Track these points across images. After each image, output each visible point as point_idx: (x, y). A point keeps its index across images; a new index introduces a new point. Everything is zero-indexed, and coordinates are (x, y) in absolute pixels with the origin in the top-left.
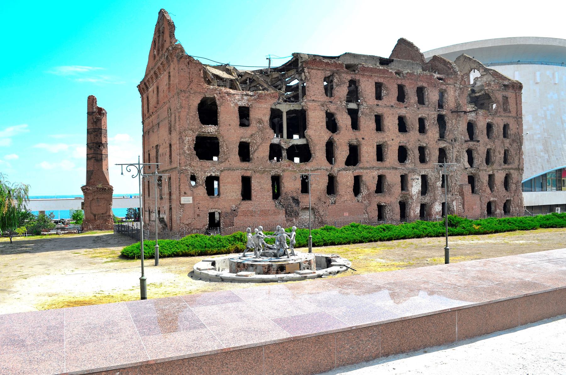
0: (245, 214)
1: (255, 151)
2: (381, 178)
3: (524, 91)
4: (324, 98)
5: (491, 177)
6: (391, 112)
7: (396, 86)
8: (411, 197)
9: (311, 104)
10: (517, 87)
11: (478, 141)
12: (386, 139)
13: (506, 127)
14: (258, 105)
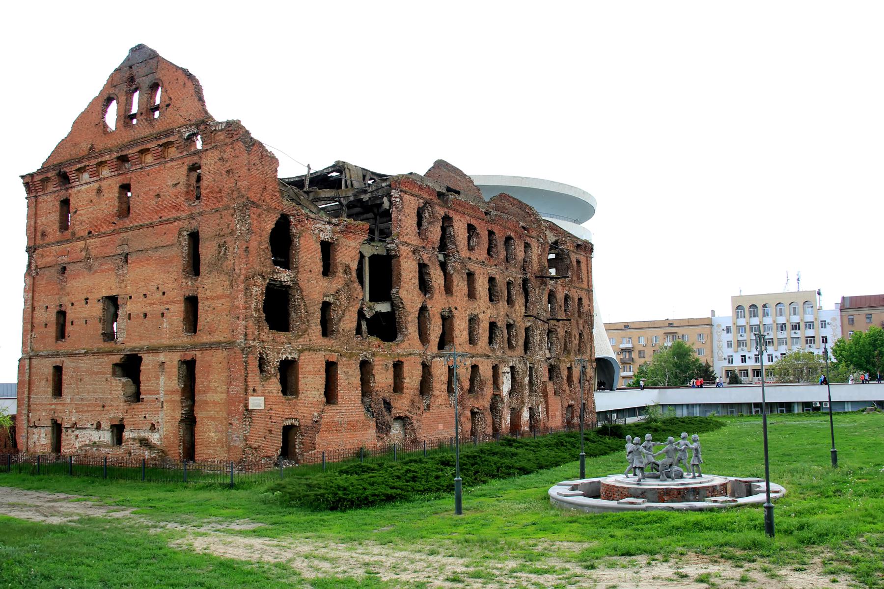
0: (335, 427)
1: (340, 320)
2: (475, 368)
3: (596, 254)
4: (415, 241)
5: (570, 369)
6: (482, 271)
7: (487, 233)
8: (502, 400)
9: (403, 247)
10: (586, 248)
11: (558, 320)
12: (478, 311)
13: (580, 299)
14: (344, 241)
